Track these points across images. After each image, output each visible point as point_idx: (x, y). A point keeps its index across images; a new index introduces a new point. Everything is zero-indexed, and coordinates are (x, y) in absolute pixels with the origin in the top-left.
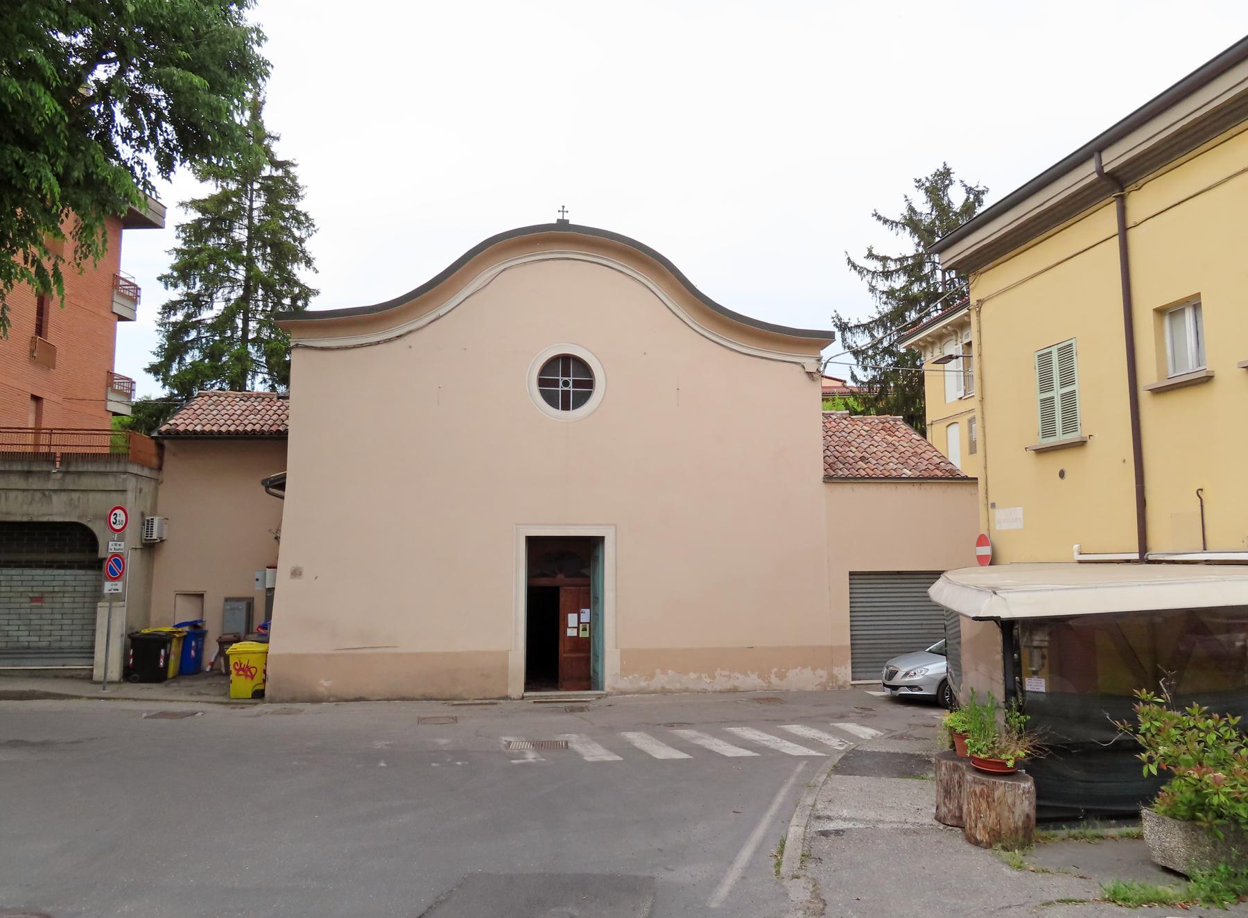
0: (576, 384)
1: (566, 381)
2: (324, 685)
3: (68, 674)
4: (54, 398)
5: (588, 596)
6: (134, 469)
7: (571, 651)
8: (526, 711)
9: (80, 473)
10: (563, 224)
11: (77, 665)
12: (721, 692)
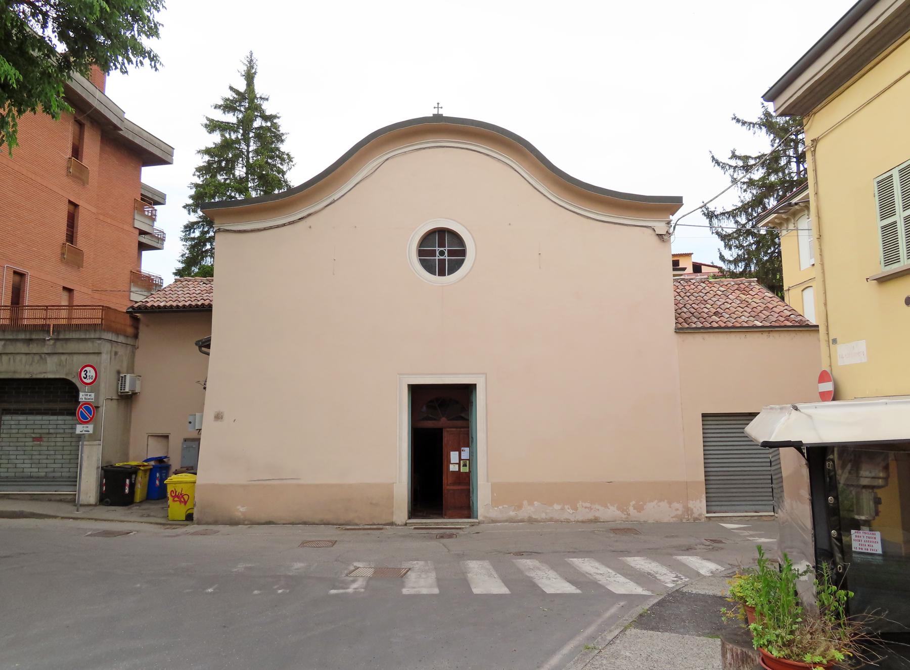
0: (451, 253)
1: (442, 250)
2: (240, 510)
3: (58, 498)
4: (84, 290)
5: (466, 438)
6: (109, 336)
7: (454, 484)
8: (404, 536)
9: (67, 340)
10: (438, 118)
11: (65, 491)
12: (583, 522)
